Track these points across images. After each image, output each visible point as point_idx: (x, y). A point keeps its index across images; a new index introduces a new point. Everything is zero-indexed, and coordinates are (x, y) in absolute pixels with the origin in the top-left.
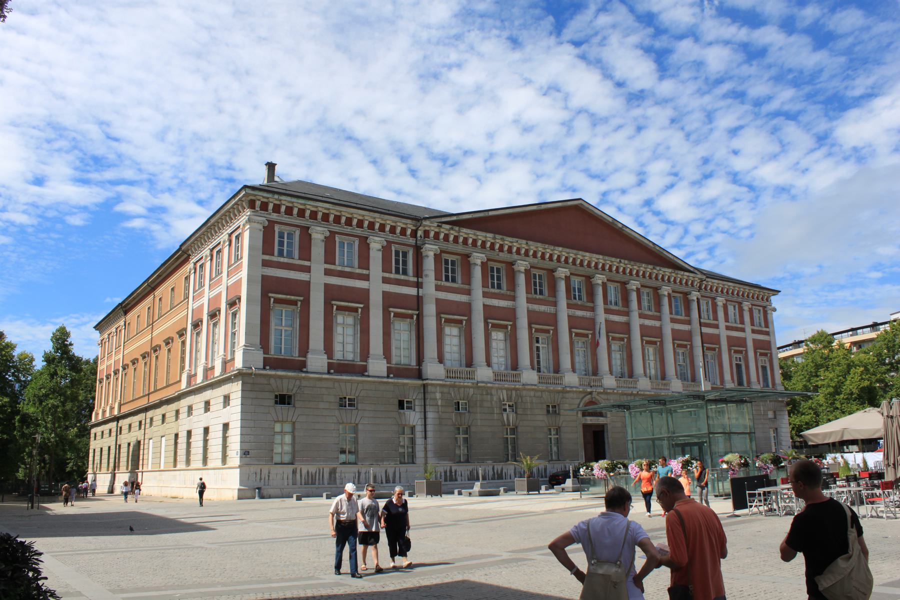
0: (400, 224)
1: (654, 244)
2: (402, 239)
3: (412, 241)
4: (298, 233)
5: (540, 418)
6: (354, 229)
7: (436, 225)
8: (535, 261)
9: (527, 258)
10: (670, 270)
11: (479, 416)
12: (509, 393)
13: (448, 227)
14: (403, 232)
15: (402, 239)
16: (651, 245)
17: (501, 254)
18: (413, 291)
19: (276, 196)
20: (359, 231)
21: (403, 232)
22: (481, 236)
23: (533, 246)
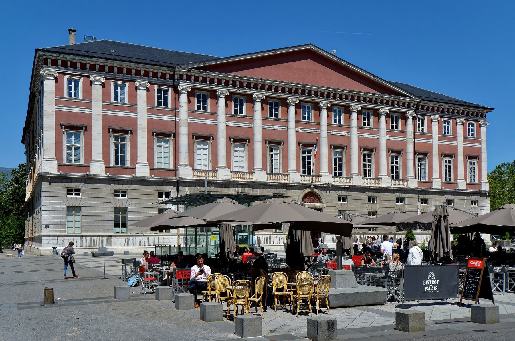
0: (160, 70)
3: (170, 82)
4: (82, 80)
6: (124, 76)
14: (163, 76)
18: (172, 118)
19: (62, 56)
20: (128, 77)
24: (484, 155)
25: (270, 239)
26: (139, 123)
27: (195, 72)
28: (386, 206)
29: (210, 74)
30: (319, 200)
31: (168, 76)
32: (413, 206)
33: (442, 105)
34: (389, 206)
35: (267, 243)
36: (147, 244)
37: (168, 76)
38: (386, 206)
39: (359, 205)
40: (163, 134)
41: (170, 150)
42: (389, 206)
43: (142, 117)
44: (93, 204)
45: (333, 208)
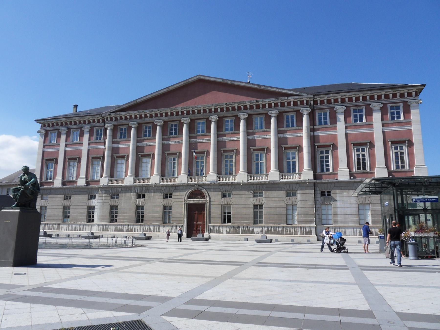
1: (258, 85)
2: (99, 124)
3: (103, 124)
5: (159, 200)
7: (108, 114)
8: (167, 118)
9: (162, 118)
10: (273, 99)
11: (123, 201)
12: (141, 188)
13: (114, 114)
15: (99, 124)
16: (256, 87)
17: (146, 119)
20: (80, 126)
21: (99, 121)
22: (133, 113)
23: (164, 111)
24: (416, 138)
25: (159, 228)
26: (83, 152)
27: (113, 115)
28: (273, 199)
29: (123, 114)
30: (204, 197)
31: (101, 120)
32: (307, 199)
33: (347, 95)
34: (277, 199)
35: (157, 232)
36: (102, 230)
37: (101, 120)
38: (273, 199)
39: (243, 199)
40: (94, 158)
41: (100, 168)
42: (277, 199)
43: (84, 149)
44: (53, 204)
45: (217, 203)
